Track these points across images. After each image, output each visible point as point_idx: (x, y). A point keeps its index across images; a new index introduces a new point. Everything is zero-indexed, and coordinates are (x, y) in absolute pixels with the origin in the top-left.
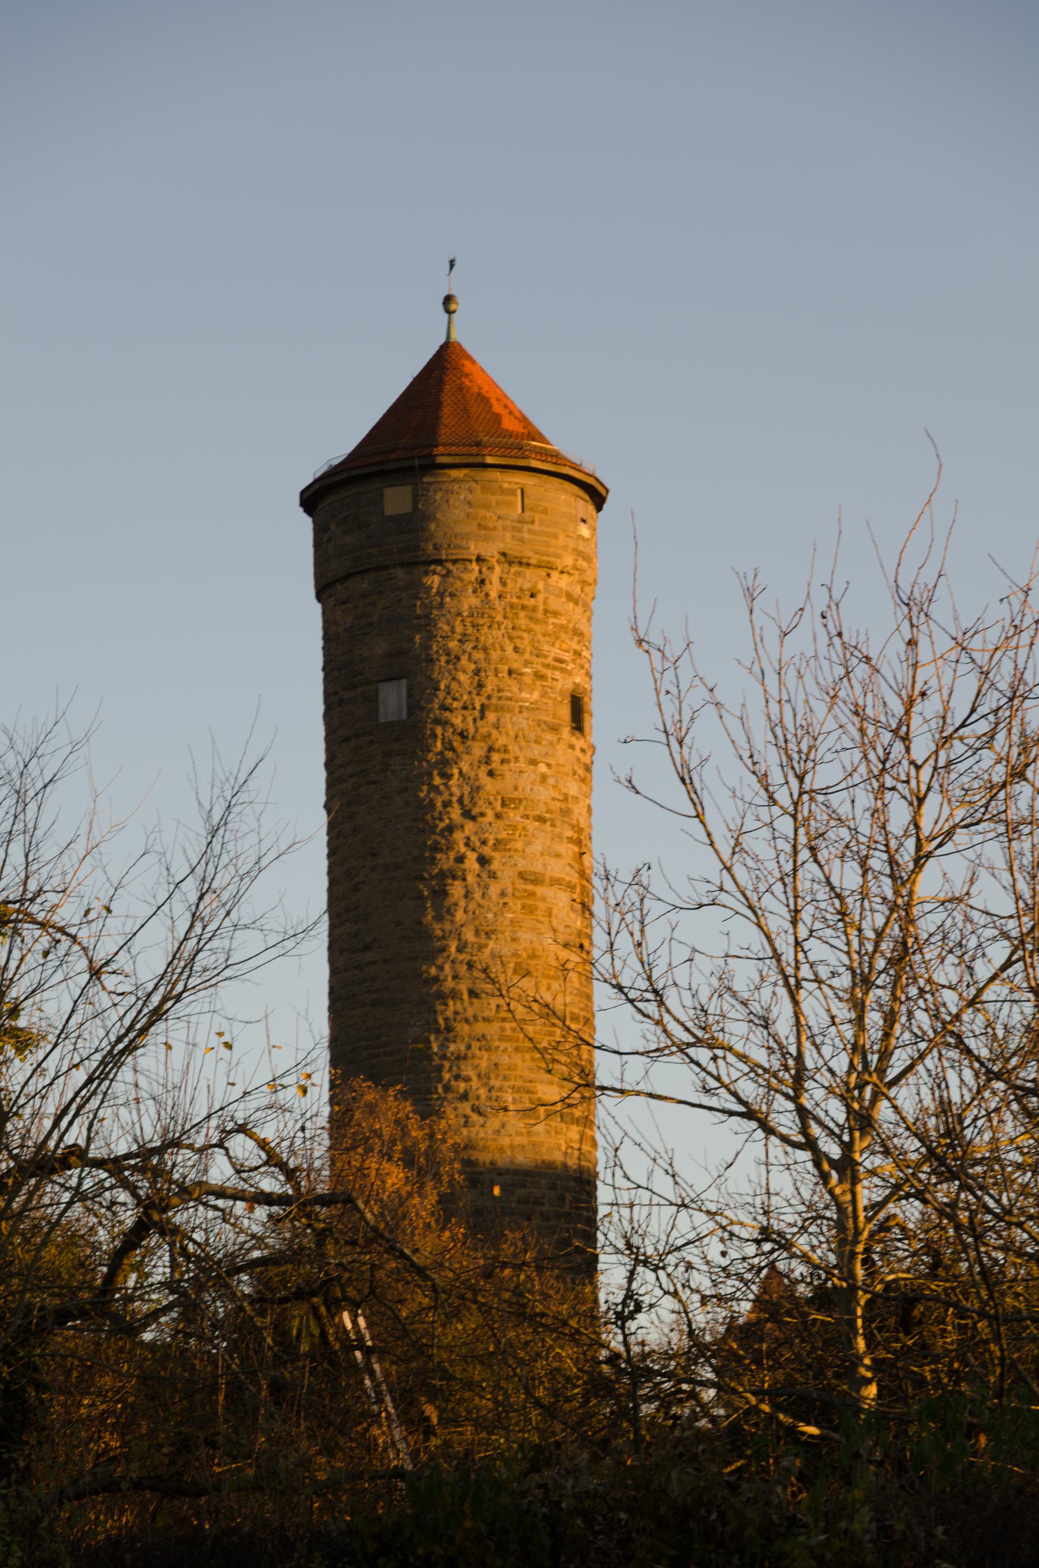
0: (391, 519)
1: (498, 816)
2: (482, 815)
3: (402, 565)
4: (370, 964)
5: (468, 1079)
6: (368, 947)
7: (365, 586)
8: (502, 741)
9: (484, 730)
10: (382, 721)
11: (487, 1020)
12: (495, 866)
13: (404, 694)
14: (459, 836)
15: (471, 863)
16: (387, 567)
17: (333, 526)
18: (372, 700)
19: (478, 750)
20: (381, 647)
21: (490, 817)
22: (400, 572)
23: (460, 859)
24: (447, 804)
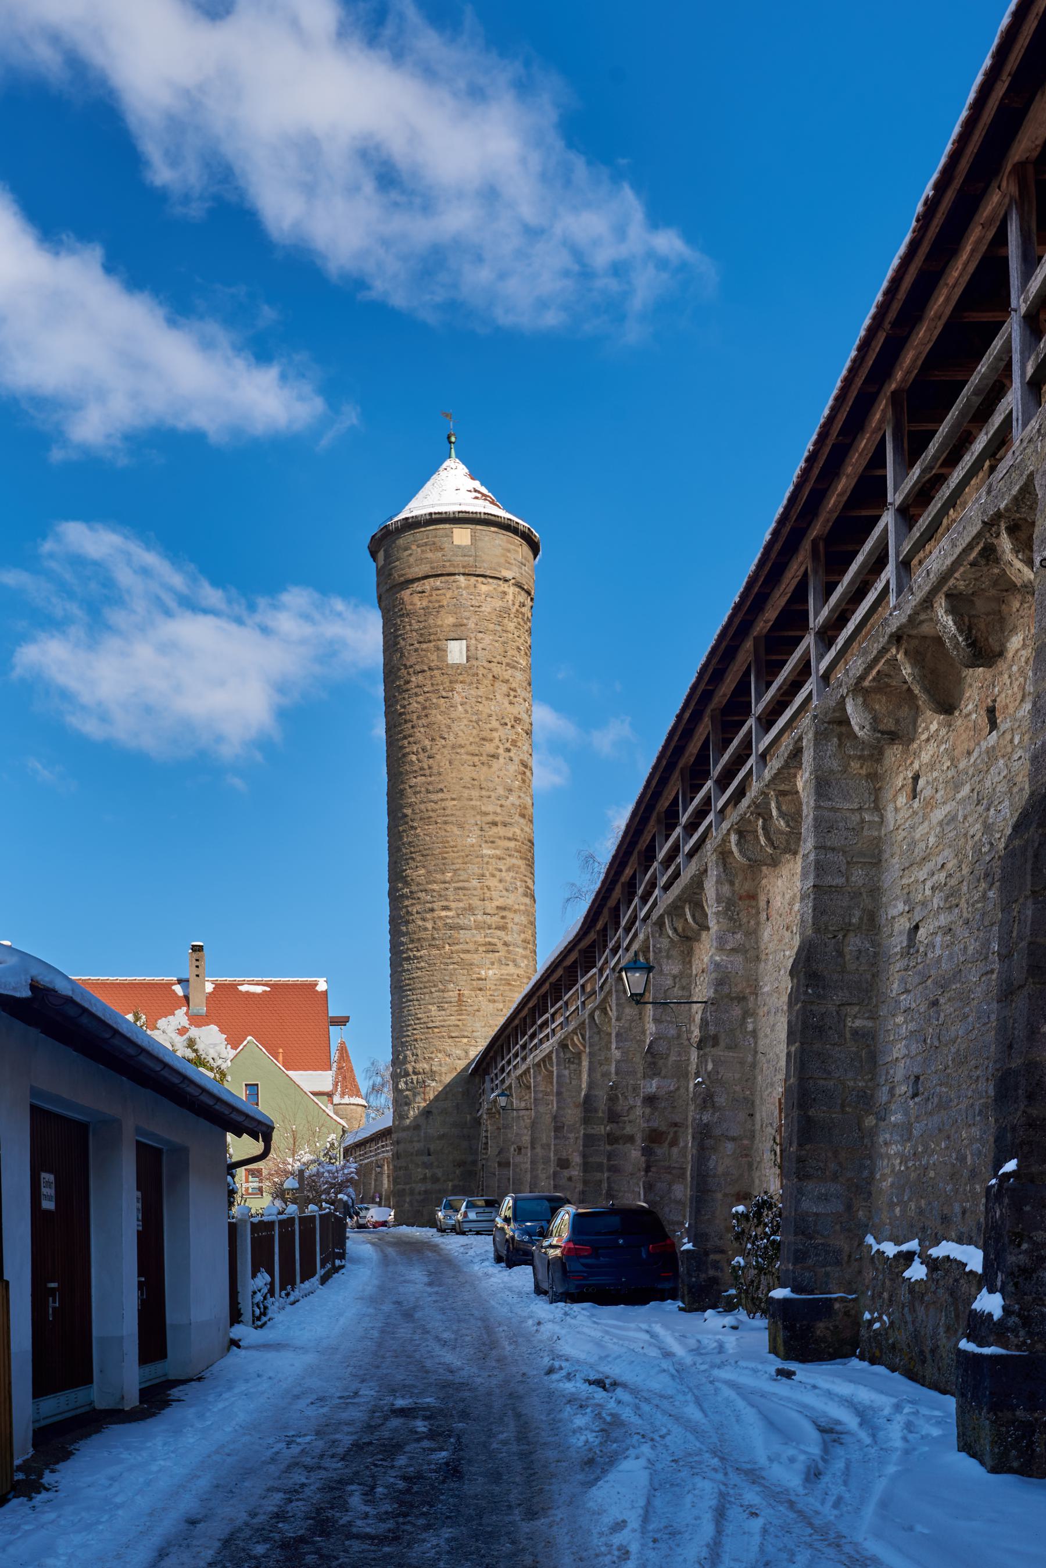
0: (459, 547)
1: (513, 726)
2: (506, 724)
3: (464, 574)
4: (442, 800)
5: (501, 870)
6: (442, 790)
7: (438, 583)
8: (514, 685)
9: (507, 677)
10: (450, 662)
11: (509, 839)
12: (512, 754)
13: (465, 649)
14: (495, 735)
15: (501, 751)
16: (454, 574)
17: (414, 547)
18: (441, 651)
19: (504, 688)
20: (451, 620)
21: (509, 727)
22: (462, 578)
23: (498, 747)
24: (490, 716)
